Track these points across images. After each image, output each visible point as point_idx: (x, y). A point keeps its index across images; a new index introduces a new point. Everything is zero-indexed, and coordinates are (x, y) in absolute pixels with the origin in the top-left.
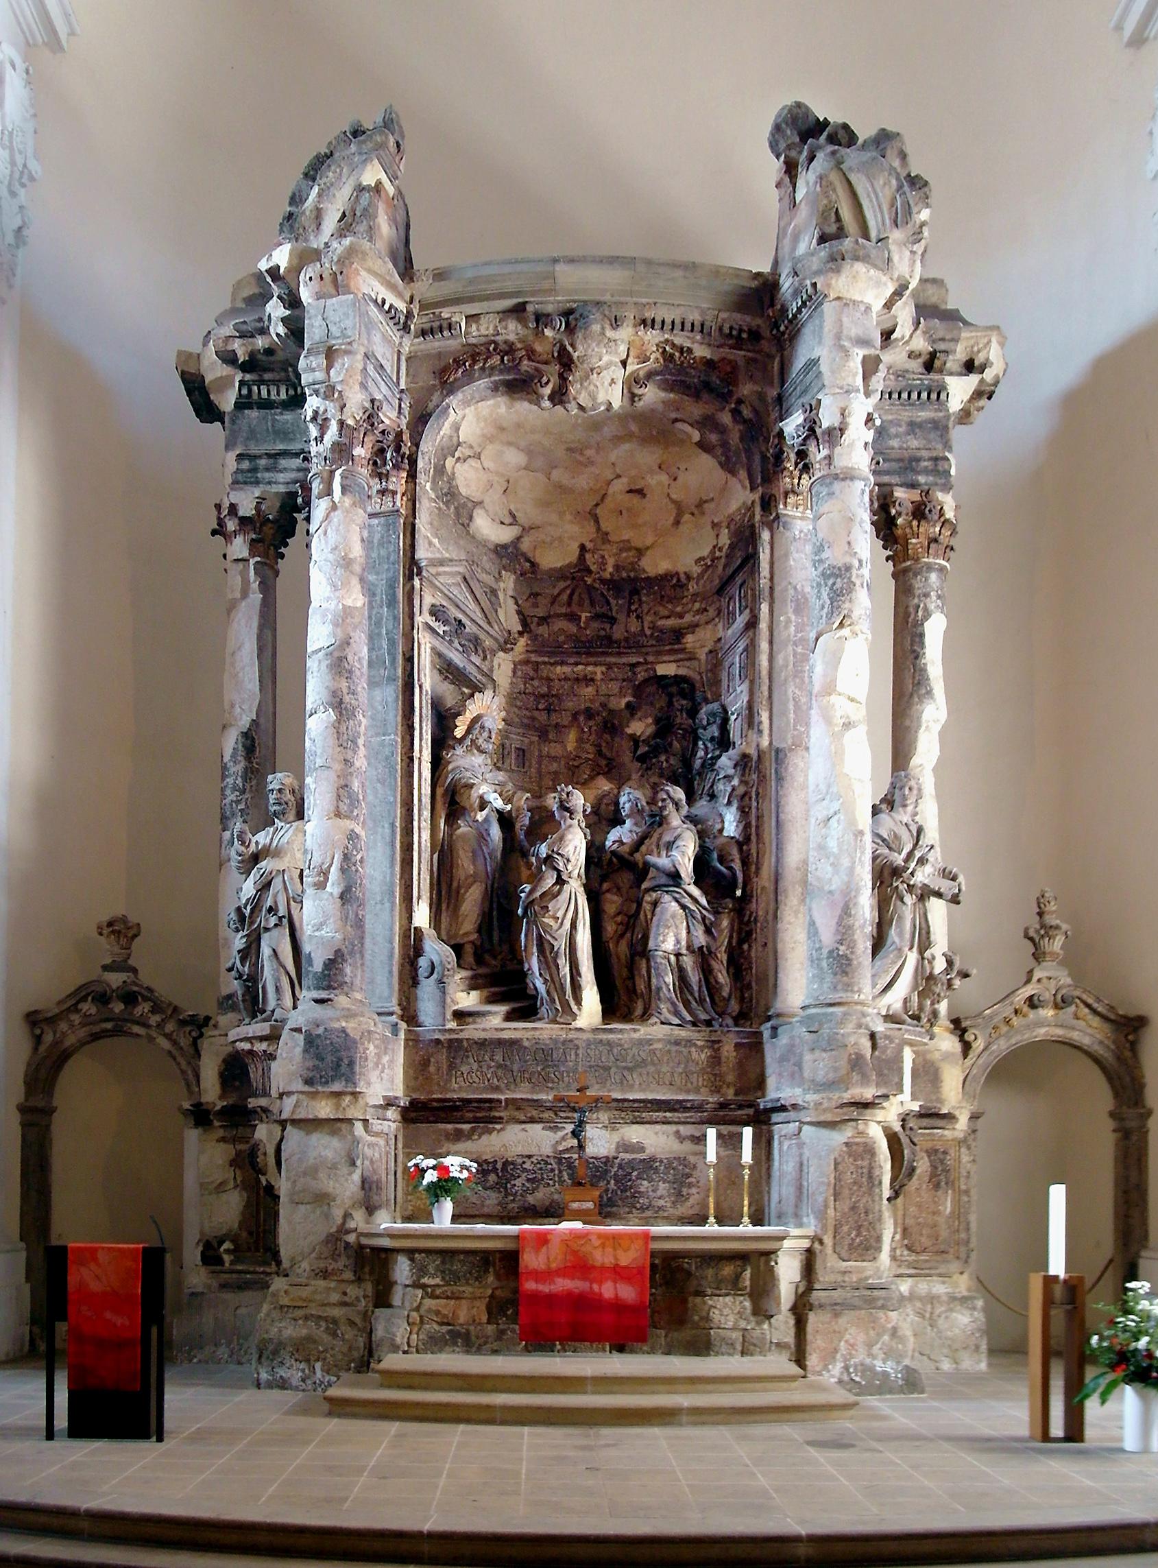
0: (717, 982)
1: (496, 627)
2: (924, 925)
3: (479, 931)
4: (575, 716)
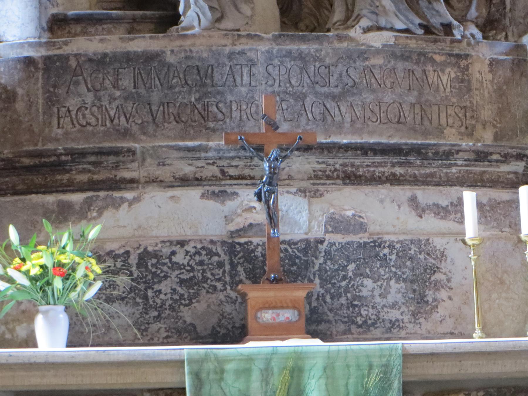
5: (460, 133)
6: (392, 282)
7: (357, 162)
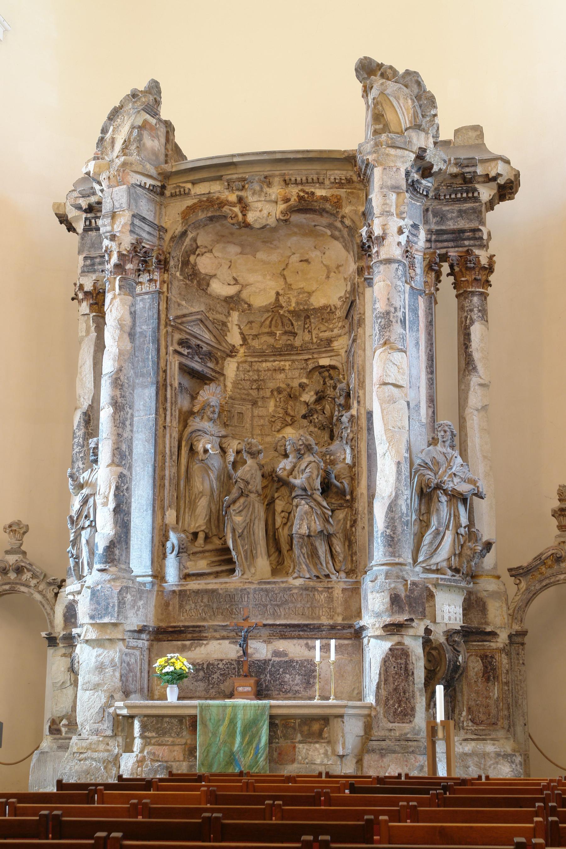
0: (336, 552)
1: (224, 344)
2: (457, 514)
3: (206, 524)
4: (272, 391)
5: (327, 618)
6: (297, 676)
7: (285, 630)
